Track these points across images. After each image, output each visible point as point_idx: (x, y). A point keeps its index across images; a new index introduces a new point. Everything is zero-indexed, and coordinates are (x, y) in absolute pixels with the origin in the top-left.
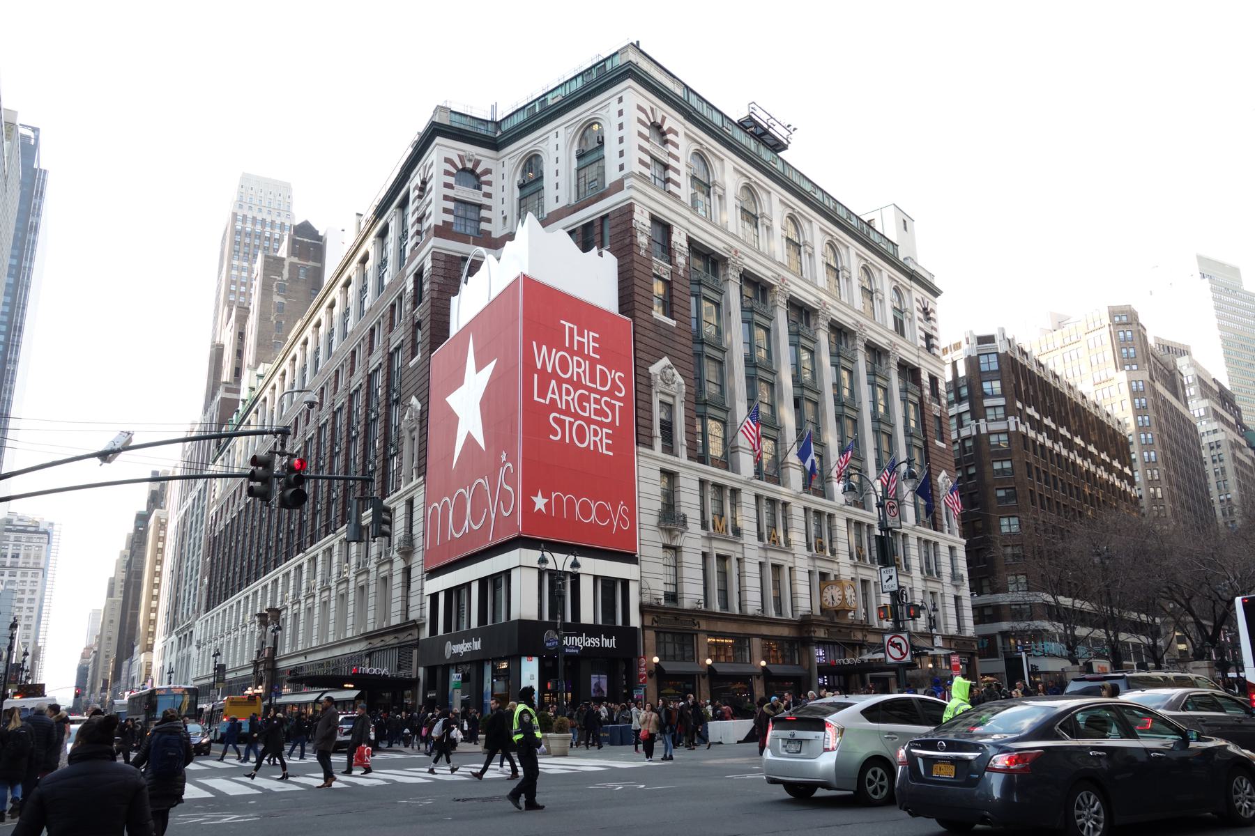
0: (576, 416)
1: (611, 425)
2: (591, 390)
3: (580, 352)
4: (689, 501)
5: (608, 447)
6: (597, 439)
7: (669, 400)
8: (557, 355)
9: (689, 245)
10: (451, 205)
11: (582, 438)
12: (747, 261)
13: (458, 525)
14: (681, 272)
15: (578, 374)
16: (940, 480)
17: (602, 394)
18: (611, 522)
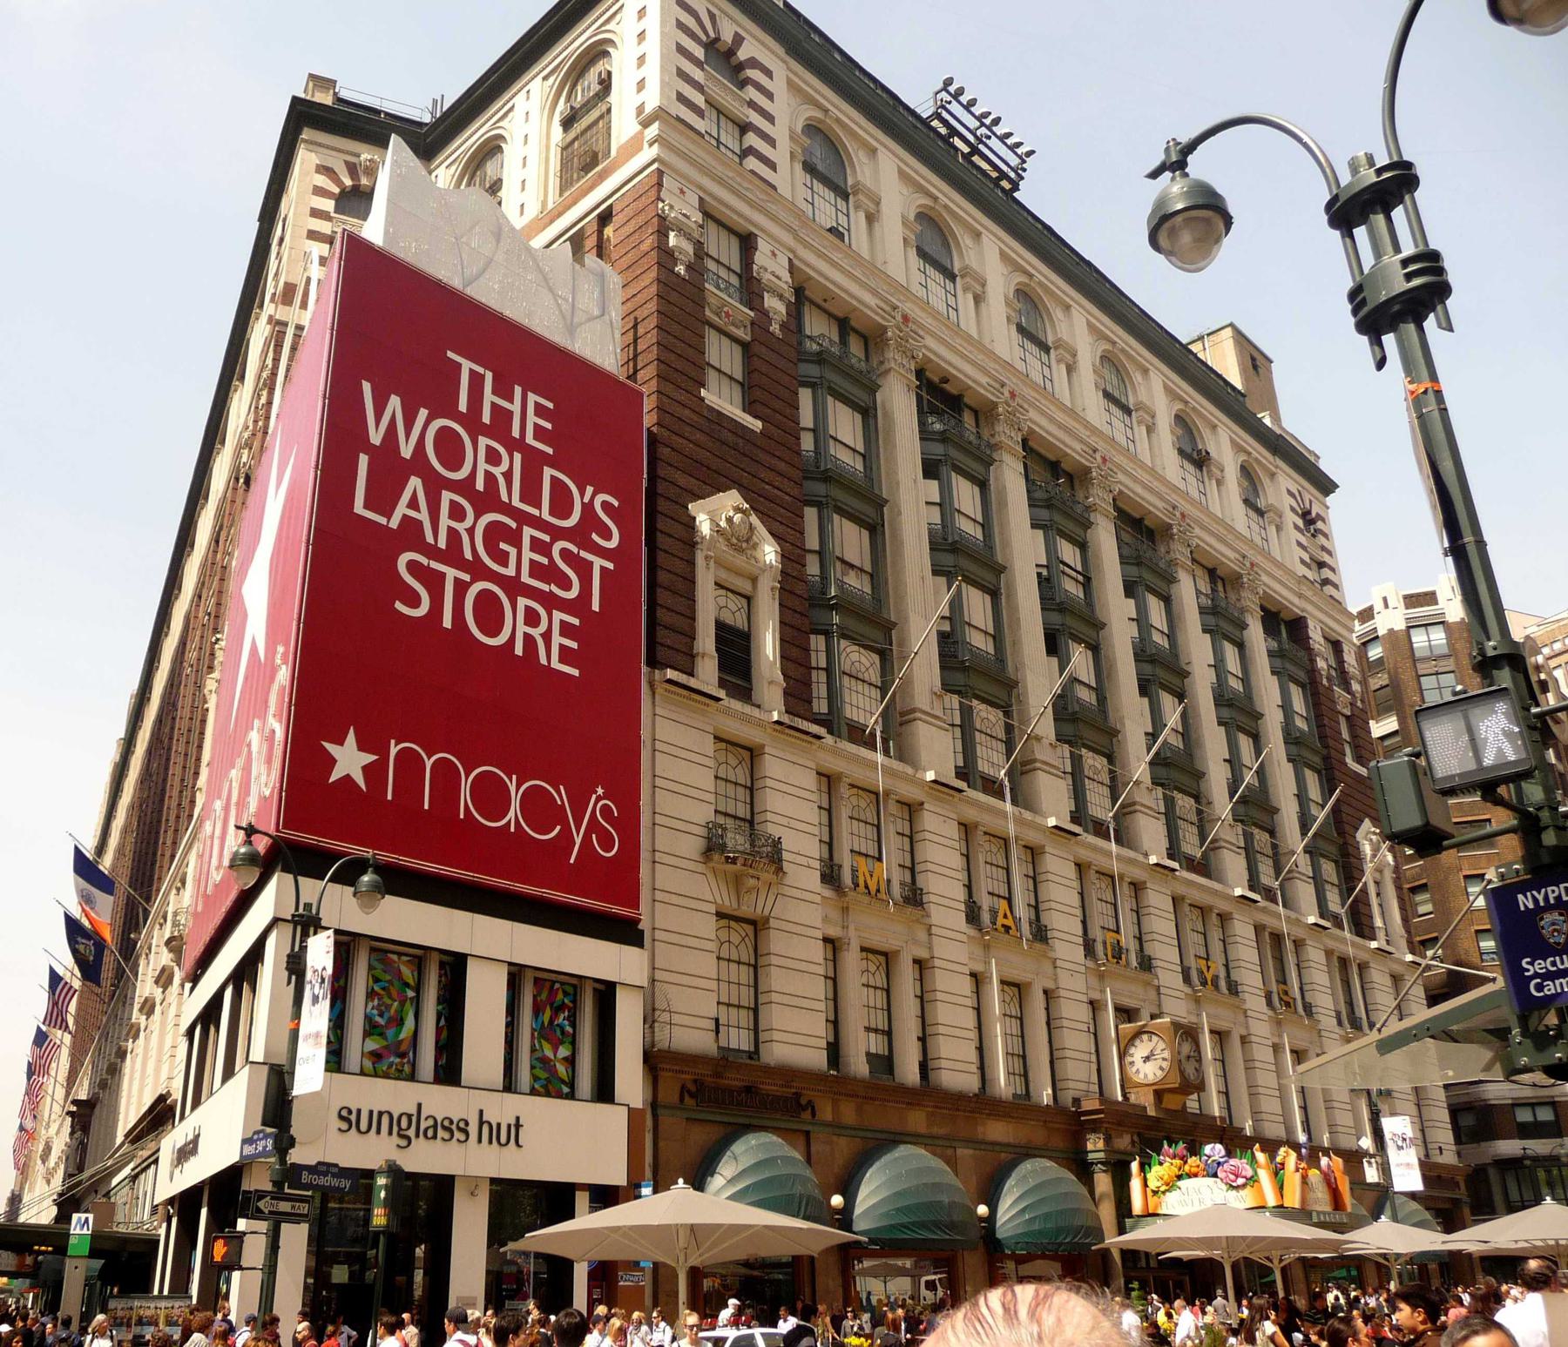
0: (478, 570)
1: (579, 606)
2: (523, 519)
4: (792, 810)
6: (536, 633)
7: (745, 586)
12: (930, 342)
14: (775, 328)
15: (489, 477)
16: (1360, 835)
17: (557, 533)
18: (566, 836)
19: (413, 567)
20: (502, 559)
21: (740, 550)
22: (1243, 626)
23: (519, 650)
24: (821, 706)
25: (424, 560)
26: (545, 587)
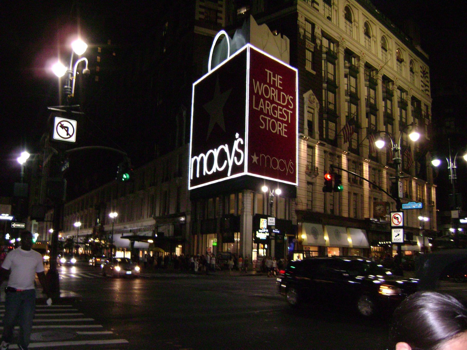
0: (272, 117)
1: (286, 122)
3: (274, 86)
5: (286, 133)
6: (280, 129)
7: (312, 111)
8: (264, 86)
9: (322, 34)
10: (203, 10)
11: (274, 129)
13: (210, 168)
14: (318, 48)
17: (283, 107)
18: (286, 170)
19: (262, 118)
20: (275, 113)
21: (312, 103)
22: (407, 105)
23: (278, 133)
24: (324, 137)
25: (263, 116)
26: (281, 119)
